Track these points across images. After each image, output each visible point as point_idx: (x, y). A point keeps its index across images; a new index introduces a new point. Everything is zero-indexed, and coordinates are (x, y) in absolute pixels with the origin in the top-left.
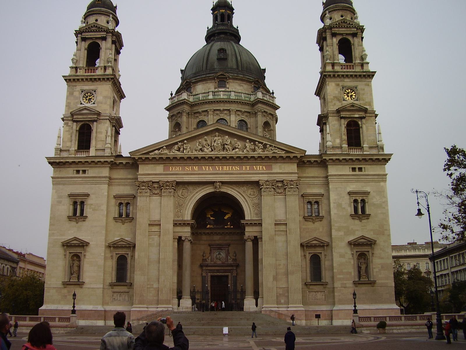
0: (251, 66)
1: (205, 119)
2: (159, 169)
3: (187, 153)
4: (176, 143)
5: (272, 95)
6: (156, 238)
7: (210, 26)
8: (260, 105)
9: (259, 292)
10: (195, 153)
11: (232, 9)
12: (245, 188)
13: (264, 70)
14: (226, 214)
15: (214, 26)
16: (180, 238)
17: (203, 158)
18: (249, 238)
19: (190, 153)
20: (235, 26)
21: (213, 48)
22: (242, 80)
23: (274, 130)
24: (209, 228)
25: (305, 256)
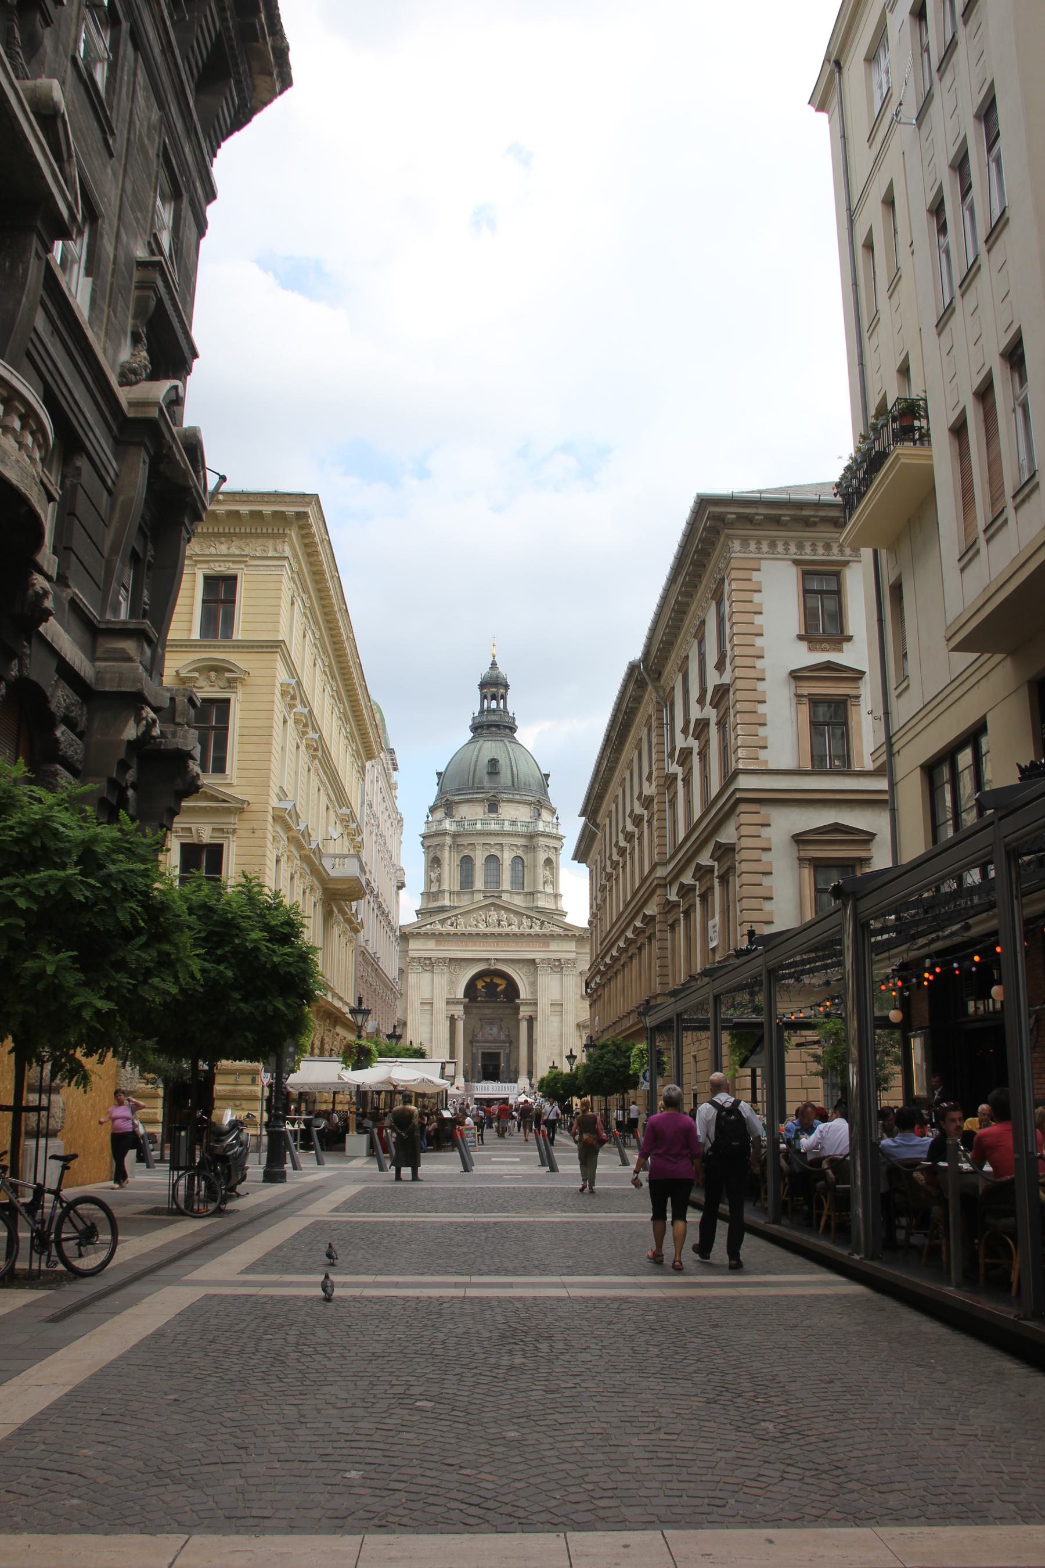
0: (531, 780)
1: (471, 854)
2: (431, 944)
3: (461, 929)
4: (449, 918)
5: (555, 821)
6: (428, 1016)
7: (476, 714)
8: (540, 838)
9: (532, 1073)
10: (469, 929)
11: (506, 687)
12: (520, 965)
13: (547, 776)
14: (498, 985)
15: (482, 712)
16: (453, 1016)
17: (478, 934)
18: (523, 1017)
19: (464, 929)
20: (510, 709)
21: (482, 753)
22: (519, 802)
23: (557, 869)
24: (481, 1001)
25: (581, 1036)
